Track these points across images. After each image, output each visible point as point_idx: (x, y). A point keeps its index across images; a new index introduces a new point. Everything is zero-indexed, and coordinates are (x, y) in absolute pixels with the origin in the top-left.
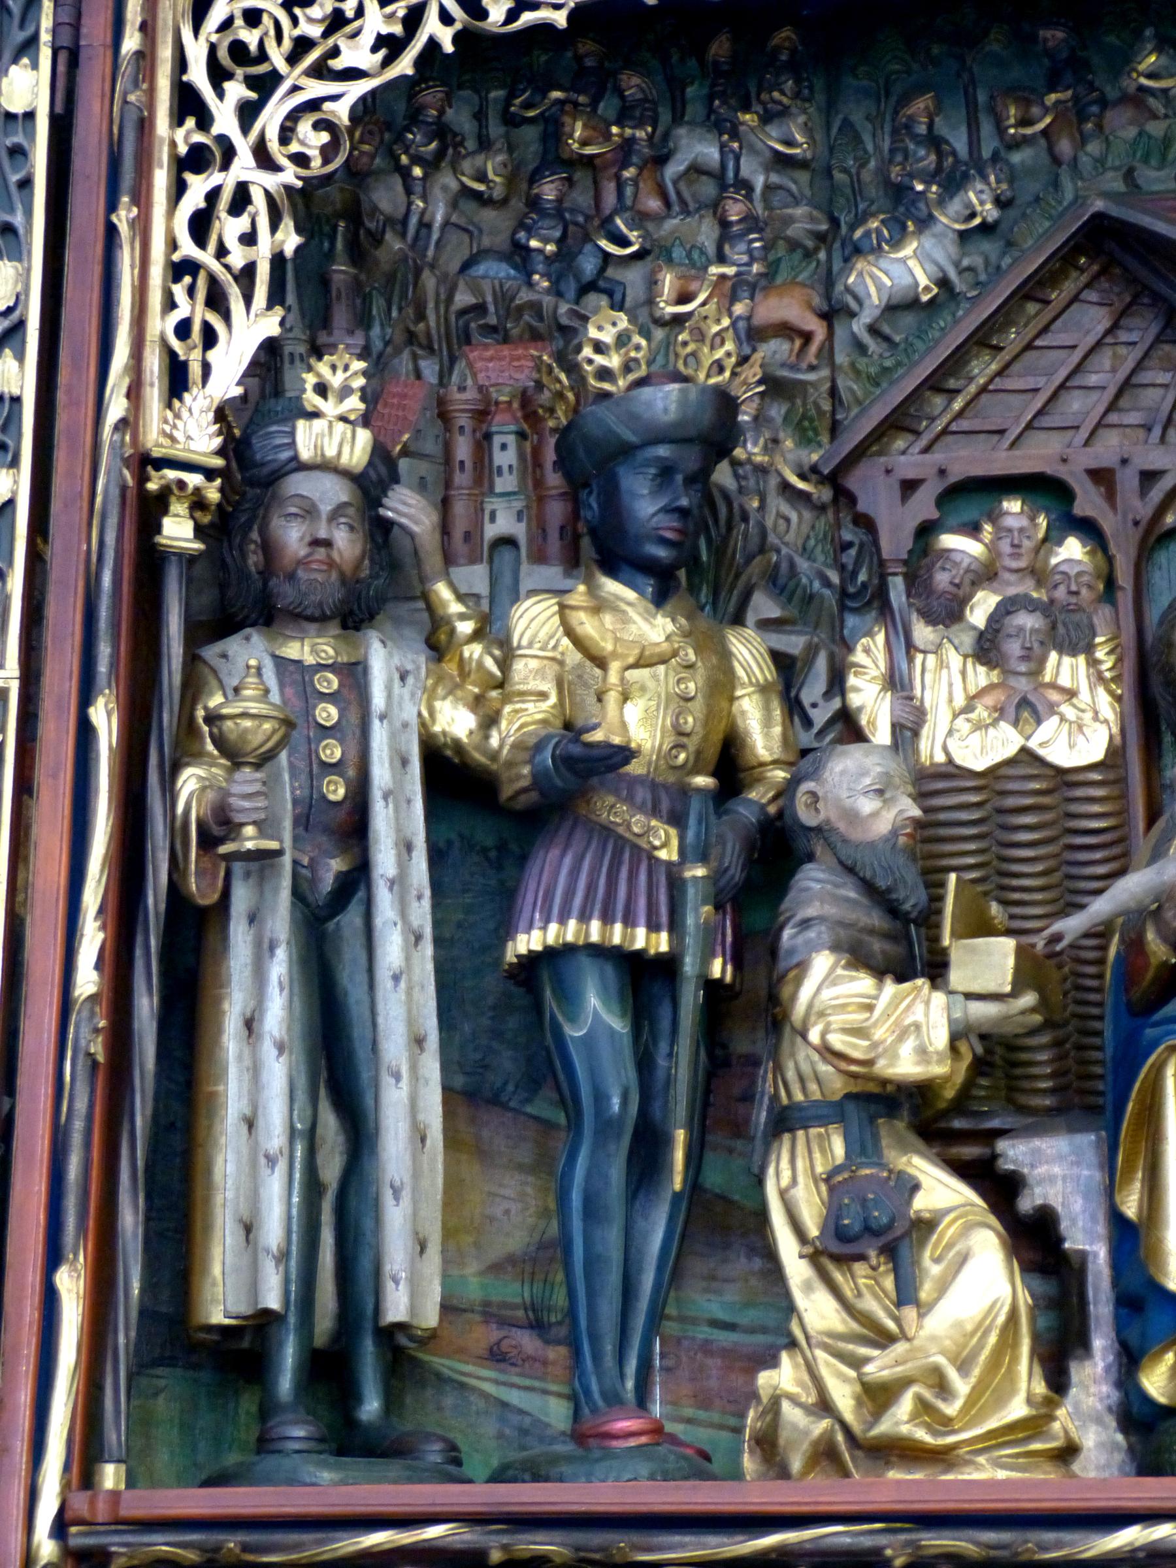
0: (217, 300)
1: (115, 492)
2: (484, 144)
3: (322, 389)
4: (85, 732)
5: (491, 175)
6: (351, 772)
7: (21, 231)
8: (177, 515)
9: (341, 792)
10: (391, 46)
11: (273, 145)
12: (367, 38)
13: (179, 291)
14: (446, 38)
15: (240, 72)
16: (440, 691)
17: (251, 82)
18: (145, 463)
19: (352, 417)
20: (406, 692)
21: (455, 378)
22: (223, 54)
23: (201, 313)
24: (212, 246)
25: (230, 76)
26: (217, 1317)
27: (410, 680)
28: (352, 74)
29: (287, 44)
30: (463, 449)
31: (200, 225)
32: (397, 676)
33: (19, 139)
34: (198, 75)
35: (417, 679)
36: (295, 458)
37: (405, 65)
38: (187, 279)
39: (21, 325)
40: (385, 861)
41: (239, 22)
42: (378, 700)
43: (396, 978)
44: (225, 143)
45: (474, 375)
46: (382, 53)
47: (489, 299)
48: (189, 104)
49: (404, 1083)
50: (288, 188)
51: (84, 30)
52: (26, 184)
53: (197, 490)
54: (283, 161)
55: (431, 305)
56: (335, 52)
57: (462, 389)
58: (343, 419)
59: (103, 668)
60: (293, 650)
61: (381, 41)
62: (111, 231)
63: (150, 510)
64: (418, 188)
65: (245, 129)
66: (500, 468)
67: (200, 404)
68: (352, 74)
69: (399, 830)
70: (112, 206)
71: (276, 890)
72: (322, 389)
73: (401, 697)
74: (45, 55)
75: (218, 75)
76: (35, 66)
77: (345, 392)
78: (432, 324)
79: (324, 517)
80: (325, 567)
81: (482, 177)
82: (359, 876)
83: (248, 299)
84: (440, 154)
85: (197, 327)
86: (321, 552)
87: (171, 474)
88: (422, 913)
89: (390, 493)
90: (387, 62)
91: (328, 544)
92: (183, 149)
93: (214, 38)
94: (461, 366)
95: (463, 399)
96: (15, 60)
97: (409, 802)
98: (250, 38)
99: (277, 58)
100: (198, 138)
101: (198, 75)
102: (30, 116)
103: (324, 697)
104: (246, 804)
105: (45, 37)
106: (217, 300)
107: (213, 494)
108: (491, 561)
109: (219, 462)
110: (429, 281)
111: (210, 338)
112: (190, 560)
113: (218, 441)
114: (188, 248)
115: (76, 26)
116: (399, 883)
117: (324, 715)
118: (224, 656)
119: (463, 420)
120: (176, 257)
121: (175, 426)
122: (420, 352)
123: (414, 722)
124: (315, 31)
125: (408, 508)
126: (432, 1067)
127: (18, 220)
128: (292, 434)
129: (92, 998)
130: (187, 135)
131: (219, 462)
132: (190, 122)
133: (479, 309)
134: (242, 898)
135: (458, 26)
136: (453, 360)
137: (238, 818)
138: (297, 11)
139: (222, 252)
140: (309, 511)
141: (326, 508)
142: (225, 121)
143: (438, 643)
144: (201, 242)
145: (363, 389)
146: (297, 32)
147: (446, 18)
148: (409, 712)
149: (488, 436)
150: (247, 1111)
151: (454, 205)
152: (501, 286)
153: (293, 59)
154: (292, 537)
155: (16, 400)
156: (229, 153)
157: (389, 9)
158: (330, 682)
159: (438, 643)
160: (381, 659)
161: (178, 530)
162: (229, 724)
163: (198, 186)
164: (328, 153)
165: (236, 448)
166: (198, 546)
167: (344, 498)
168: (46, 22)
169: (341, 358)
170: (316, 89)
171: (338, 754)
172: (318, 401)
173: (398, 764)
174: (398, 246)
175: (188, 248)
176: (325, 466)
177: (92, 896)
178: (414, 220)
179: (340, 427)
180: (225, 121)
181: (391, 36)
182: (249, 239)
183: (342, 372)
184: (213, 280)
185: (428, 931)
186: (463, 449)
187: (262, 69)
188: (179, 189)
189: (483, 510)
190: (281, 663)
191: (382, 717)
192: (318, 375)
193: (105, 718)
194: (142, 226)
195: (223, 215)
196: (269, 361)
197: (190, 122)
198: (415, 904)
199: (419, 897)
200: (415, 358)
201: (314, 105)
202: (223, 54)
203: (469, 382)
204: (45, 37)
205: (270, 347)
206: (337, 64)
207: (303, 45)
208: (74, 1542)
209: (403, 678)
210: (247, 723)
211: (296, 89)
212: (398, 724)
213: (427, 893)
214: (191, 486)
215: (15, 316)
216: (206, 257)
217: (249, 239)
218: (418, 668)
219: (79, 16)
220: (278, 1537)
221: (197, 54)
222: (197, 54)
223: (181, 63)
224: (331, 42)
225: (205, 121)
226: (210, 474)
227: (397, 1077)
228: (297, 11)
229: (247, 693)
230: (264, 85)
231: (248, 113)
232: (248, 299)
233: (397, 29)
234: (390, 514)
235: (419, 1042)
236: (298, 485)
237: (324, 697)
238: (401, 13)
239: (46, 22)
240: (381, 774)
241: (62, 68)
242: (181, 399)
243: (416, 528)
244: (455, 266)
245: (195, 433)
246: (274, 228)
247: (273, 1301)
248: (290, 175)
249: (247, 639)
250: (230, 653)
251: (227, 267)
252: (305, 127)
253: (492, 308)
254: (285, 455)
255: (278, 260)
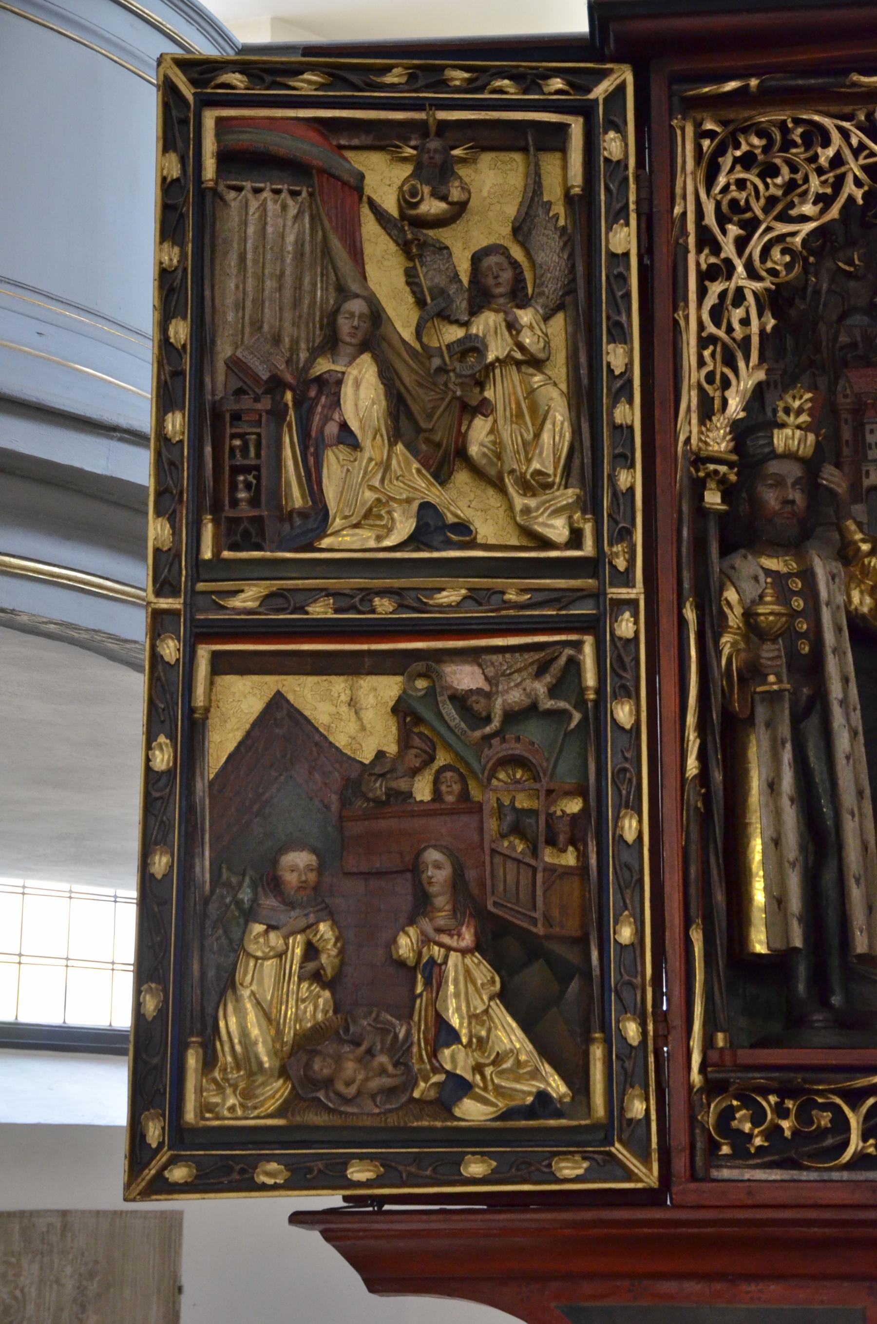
0: (730, 361)
1: (685, 480)
2: (851, 243)
3: (787, 411)
4: (682, 622)
5: (857, 262)
6: (811, 636)
7: (626, 326)
8: (711, 489)
9: (807, 649)
10: (824, 201)
11: (757, 263)
12: (811, 197)
13: (707, 353)
14: (859, 194)
15: (735, 219)
16: (853, 586)
17: (742, 225)
18: (699, 460)
19: (804, 426)
20: (836, 587)
21: (839, 388)
22: (725, 207)
23: (722, 369)
24: (724, 327)
25: (730, 221)
26: (760, 947)
27: (837, 580)
28: (804, 219)
29: (762, 201)
30: (847, 434)
31: (717, 314)
32: (830, 578)
33: (621, 269)
34: (710, 220)
35: (840, 579)
36: (773, 451)
37: (834, 212)
38: (711, 348)
39: (630, 382)
40: (836, 690)
41: (733, 187)
42: (824, 594)
43: (848, 758)
44: (728, 262)
45: (851, 387)
46: (821, 205)
47: (859, 339)
48: (707, 240)
49: (856, 818)
50: (767, 290)
51: (655, 202)
52: (627, 296)
53: (725, 474)
54: (764, 274)
55: (824, 343)
56: (792, 205)
57: (846, 396)
58: (798, 427)
59: (686, 585)
60: (772, 564)
61: (819, 198)
62: (676, 322)
63: (698, 487)
64: (812, 270)
65: (740, 254)
66: (870, 445)
67: (720, 422)
68: (804, 219)
69: (841, 671)
70: (675, 309)
71: (783, 711)
72: (787, 411)
73: (834, 590)
74: (633, 217)
75: (722, 220)
76: (627, 224)
77: (799, 412)
78: (825, 356)
79: (789, 485)
80: (790, 516)
81: (851, 263)
82: (820, 696)
83: (747, 359)
84: (823, 247)
85: (718, 377)
86: (788, 508)
87: (712, 467)
88: (856, 718)
89: (823, 469)
90: (823, 212)
91: (793, 502)
92: (704, 267)
93: (719, 197)
94: (842, 382)
95: (844, 402)
96: (615, 221)
97: (845, 653)
98: (742, 196)
99: (757, 208)
100: (713, 260)
101: (710, 220)
102: (626, 255)
103: (795, 593)
104: (769, 663)
105: (632, 206)
106: (730, 361)
107: (733, 478)
108: (866, 502)
109: (734, 458)
110: (823, 329)
111: (726, 384)
112: (720, 515)
113: (732, 444)
114: (711, 329)
115: (651, 201)
116: (844, 703)
117: (796, 604)
118: (733, 567)
119: (845, 415)
120: (704, 334)
121: (708, 436)
122: (817, 372)
123: (842, 605)
124: (779, 193)
125: (833, 478)
126: (868, 807)
127: (624, 319)
128: (772, 437)
129: (695, 776)
130: (706, 259)
131: (734, 458)
132: (706, 251)
133: (854, 345)
134: (761, 713)
135: (866, 188)
136: (837, 378)
137: (766, 671)
138: (769, 180)
139: (730, 330)
140: (779, 482)
141: (790, 482)
142: (729, 250)
143: (846, 555)
144: (718, 325)
145: (810, 409)
146: (767, 194)
147: (858, 183)
148: (840, 599)
149: (862, 425)
150: (774, 836)
151: (832, 280)
152: (866, 331)
153: (766, 210)
154: (771, 498)
155: (631, 428)
156: (729, 269)
157: (823, 178)
158: (797, 584)
159: (846, 555)
160: (821, 569)
161: (713, 498)
162: (762, 618)
163: (715, 288)
164: (789, 267)
165: (739, 447)
166: (723, 507)
167: (799, 474)
168: (632, 197)
169: (799, 391)
170: (783, 228)
171: (805, 626)
172: (785, 418)
173: (837, 632)
174: (803, 307)
175: (711, 329)
176: (790, 456)
177: (691, 719)
178: (810, 290)
179: (798, 433)
180: (729, 250)
181: (825, 194)
182: (745, 322)
183: (800, 399)
184: (725, 346)
185: (860, 729)
186: (847, 434)
187: (748, 215)
188: (702, 293)
189: (861, 470)
190: (768, 572)
191: (827, 604)
192: (786, 402)
193: (690, 614)
194: (687, 318)
195: (730, 307)
196: (758, 398)
197: (706, 251)
198: (852, 713)
199: (855, 709)
200: (814, 375)
201: (781, 238)
202: (725, 207)
203: (848, 391)
204: (632, 206)
205: (759, 386)
206: (793, 212)
207: (772, 201)
208: (710, 1076)
209: (833, 579)
210: (771, 618)
211: (769, 229)
212: (834, 607)
213: (859, 707)
214: (722, 473)
215: (625, 377)
216: (721, 333)
217: (745, 322)
218: (840, 571)
219: (651, 193)
220: (821, 1076)
221: (709, 208)
222: (709, 208)
223: (700, 214)
224: (789, 198)
225: (716, 248)
226: (731, 465)
227: (853, 815)
228: (769, 180)
229: (768, 599)
230: (750, 226)
231: (741, 244)
232: (747, 359)
233: (829, 191)
234: (824, 482)
235: (860, 793)
236: (774, 467)
237: (795, 593)
238: (831, 180)
239: (632, 197)
240: (829, 637)
241: (643, 226)
242: (711, 420)
243: (840, 490)
244: (835, 317)
245: (719, 441)
246: (760, 315)
247: (798, 943)
248: (767, 284)
249: (745, 557)
250: (736, 566)
251: (734, 339)
252: (776, 253)
253: (861, 345)
254: (767, 450)
255: (762, 332)
